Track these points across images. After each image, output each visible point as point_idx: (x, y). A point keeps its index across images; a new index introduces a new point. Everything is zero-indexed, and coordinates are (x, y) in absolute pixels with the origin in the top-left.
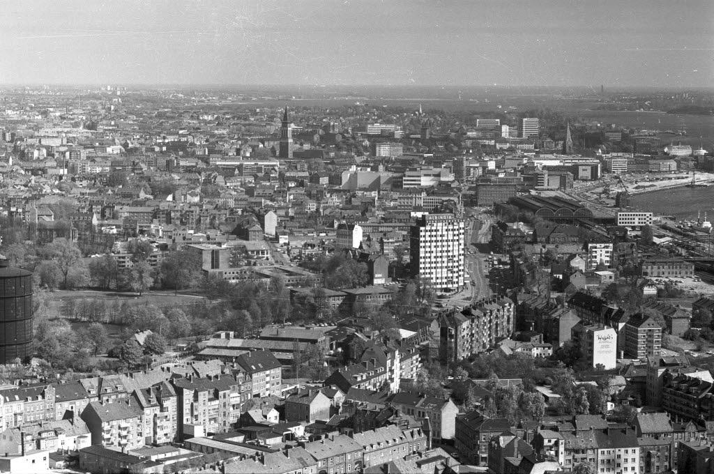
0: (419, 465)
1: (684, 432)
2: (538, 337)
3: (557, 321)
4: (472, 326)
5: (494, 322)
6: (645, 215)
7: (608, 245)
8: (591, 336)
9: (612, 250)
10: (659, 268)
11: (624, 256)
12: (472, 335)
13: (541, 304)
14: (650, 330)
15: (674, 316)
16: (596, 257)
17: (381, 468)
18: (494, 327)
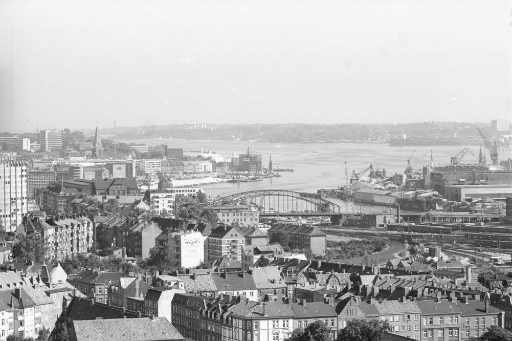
0: (48, 294)
1: (296, 284)
2: (120, 250)
3: (139, 235)
4: (56, 234)
5: (75, 236)
6: (194, 191)
7: (170, 194)
8: (177, 241)
9: (174, 200)
10: (223, 215)
11: (186, 205)
12: (56, 244)
13: (120, 222)
14: (234, 241)
15: (254, 235)
16: (158, 207)
17: (12, 293)
18: (75, 242)
